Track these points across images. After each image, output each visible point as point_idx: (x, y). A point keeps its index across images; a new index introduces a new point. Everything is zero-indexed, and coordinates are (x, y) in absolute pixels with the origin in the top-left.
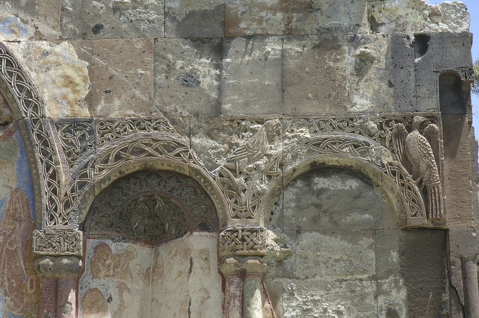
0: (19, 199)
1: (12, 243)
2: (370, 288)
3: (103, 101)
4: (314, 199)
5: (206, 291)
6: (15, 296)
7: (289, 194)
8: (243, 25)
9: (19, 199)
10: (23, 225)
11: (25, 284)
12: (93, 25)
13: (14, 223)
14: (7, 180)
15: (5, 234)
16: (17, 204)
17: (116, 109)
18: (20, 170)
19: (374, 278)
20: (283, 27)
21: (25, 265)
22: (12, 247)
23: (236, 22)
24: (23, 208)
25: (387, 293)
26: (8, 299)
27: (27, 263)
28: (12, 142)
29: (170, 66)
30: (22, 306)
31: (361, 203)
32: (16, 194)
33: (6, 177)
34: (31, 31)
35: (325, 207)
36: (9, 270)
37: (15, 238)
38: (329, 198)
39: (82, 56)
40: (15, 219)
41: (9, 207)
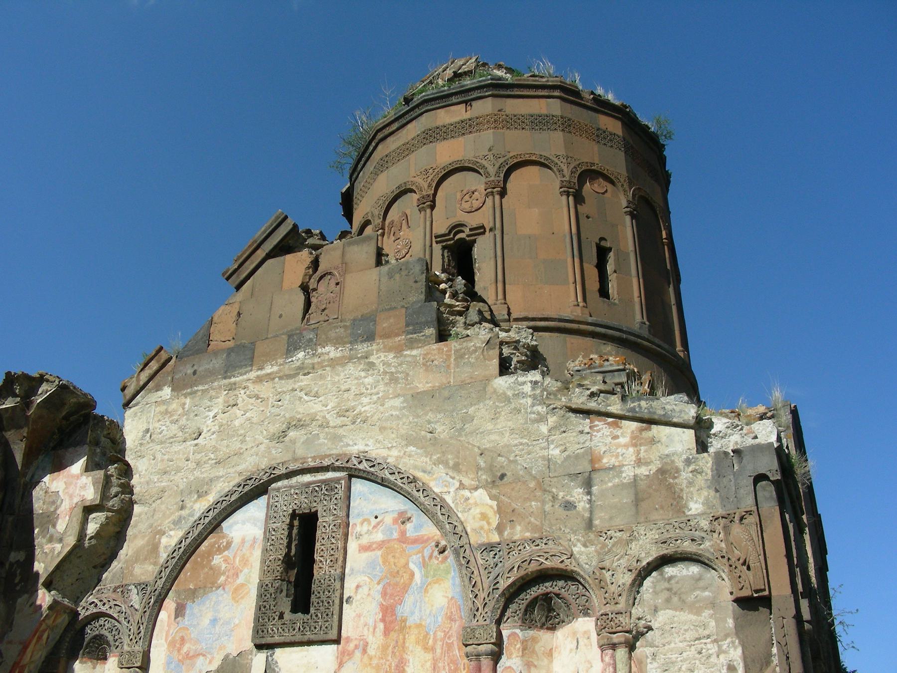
2: (713, 649)
4: (666, 585)
5: (589, 662)
7: (648, 582)
8: (605, 461)
17: (519, 532)
18: (454, 585)
19: (716, 641)
20: (634, 458)
23: (600, 459)
25: (725, 652)
29: (554, 498)
31: (701, 584)
34: (457, 484)
35: (675, 590)
38: (677, 583)
39: (492, 497)
40: (451, 619)
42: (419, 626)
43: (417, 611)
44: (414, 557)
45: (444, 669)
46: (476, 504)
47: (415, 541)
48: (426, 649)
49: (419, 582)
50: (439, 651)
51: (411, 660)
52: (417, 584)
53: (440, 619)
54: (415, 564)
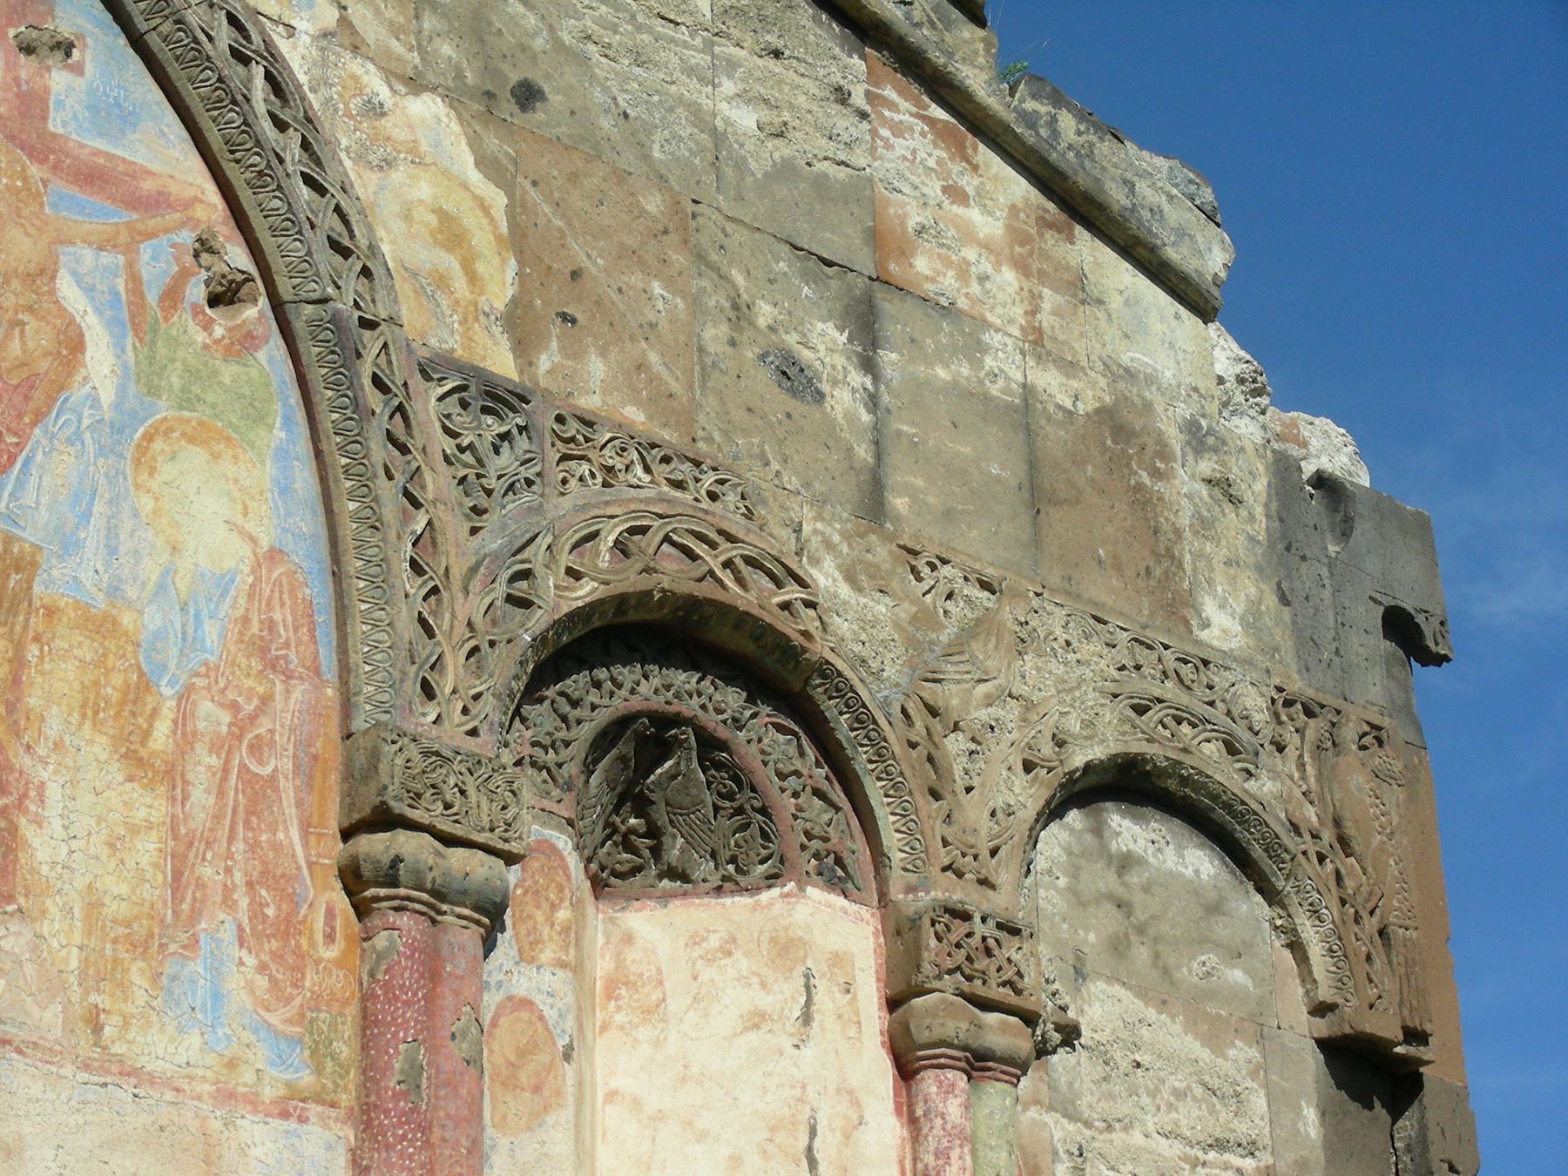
0: (281, 592)
1: (260, 748)
3: (554, 344)
6: (277, 956)
9: (281, 592)
10: (297, 695)
11: (306, 916)
12: (514, 77)
13: (266, 677)
14: (240, 507)
15: (234, 707)
16: (277, 607)
21: (306, 845)
22: (261, 763)
24: (296, 631)
26: (251, 961)
27: (312, 839)
28: (254, 373)
30: (298, 1001)
32: (270, 571)
33: (237, 495)
35: (1140, 915)
36: (254, 846)
37: (272, 732)
41: (247, 610)
42: (102, 626)
43: (92, 537)
44: (88, 255)
45: (228, 902)
46: (418, 162)
47: (94, 177)
48: (135, 760)
49: (107, 396)
50: (201, 797)
51: (53, 792)
52: (95, 403)
53: (211, 632)
54: (89, 290)
